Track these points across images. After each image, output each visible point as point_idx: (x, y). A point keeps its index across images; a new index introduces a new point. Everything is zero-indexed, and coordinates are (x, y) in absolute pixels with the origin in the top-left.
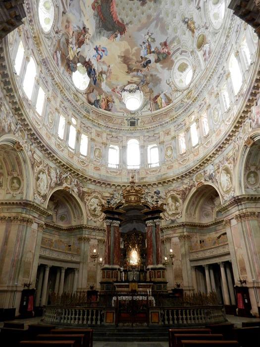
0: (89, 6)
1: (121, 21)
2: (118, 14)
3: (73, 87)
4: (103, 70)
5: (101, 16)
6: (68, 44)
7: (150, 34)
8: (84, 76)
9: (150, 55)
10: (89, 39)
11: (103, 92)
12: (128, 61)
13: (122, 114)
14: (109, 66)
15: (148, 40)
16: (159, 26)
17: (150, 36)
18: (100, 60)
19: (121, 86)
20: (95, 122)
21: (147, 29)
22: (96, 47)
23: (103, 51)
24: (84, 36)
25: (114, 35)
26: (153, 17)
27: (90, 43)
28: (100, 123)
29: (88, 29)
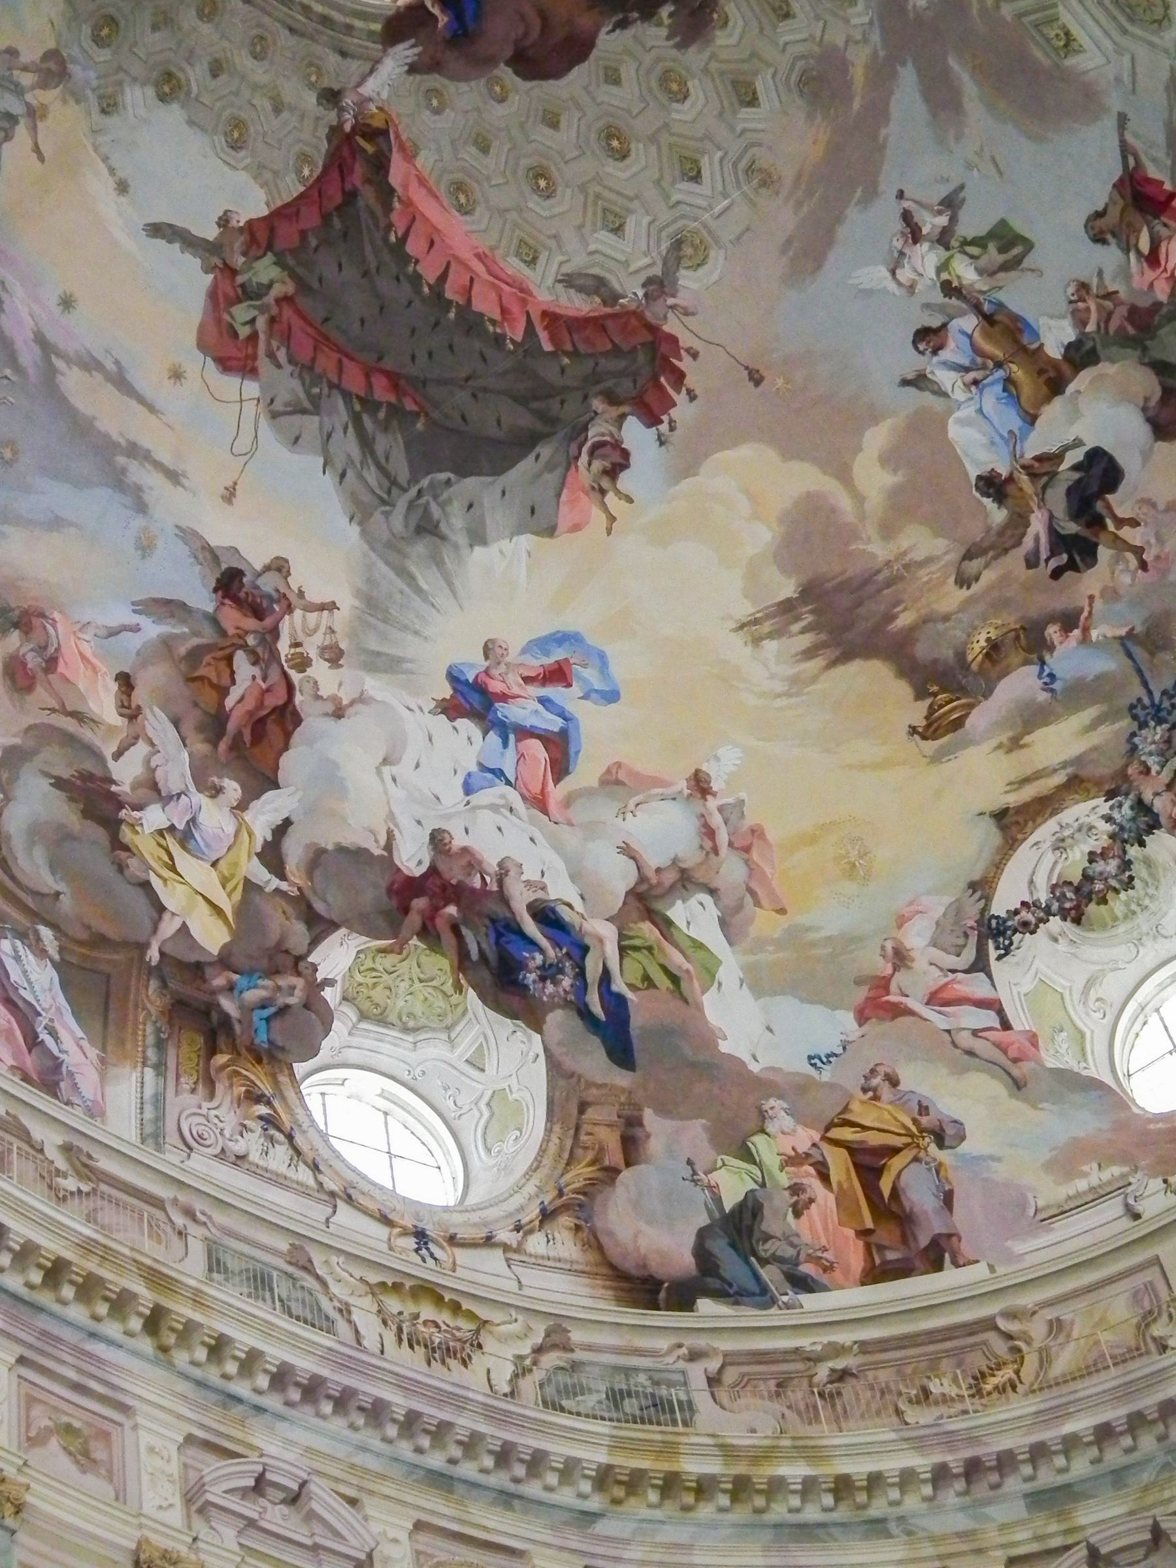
0: (177, 375)
1: (578, 305)
2: (514, 266)
3: (345, 1216)
4: (654, 859)
5: (354, 381)
6: (112, 825)
7: (932, 223)
8: (468, 1039)
9: (1058, 403)
10: (334, 656)
11: (765, 1086)
12: (873, 608)
13: (1113, 1208)
14: (700, 786)
15: (949, 289)
16: (970, 89)
17: (943, 239)
18: (569, 784)
19: (938, 906)
20: (776, 1486)
21: (872, 193)
22: (453, 677)
23: (558, 675)
24: (266, 655)
25: (586, 470)
26: (859, 60)
27: (373, 685)
28: (859, 1468)
29: (280, 567)
